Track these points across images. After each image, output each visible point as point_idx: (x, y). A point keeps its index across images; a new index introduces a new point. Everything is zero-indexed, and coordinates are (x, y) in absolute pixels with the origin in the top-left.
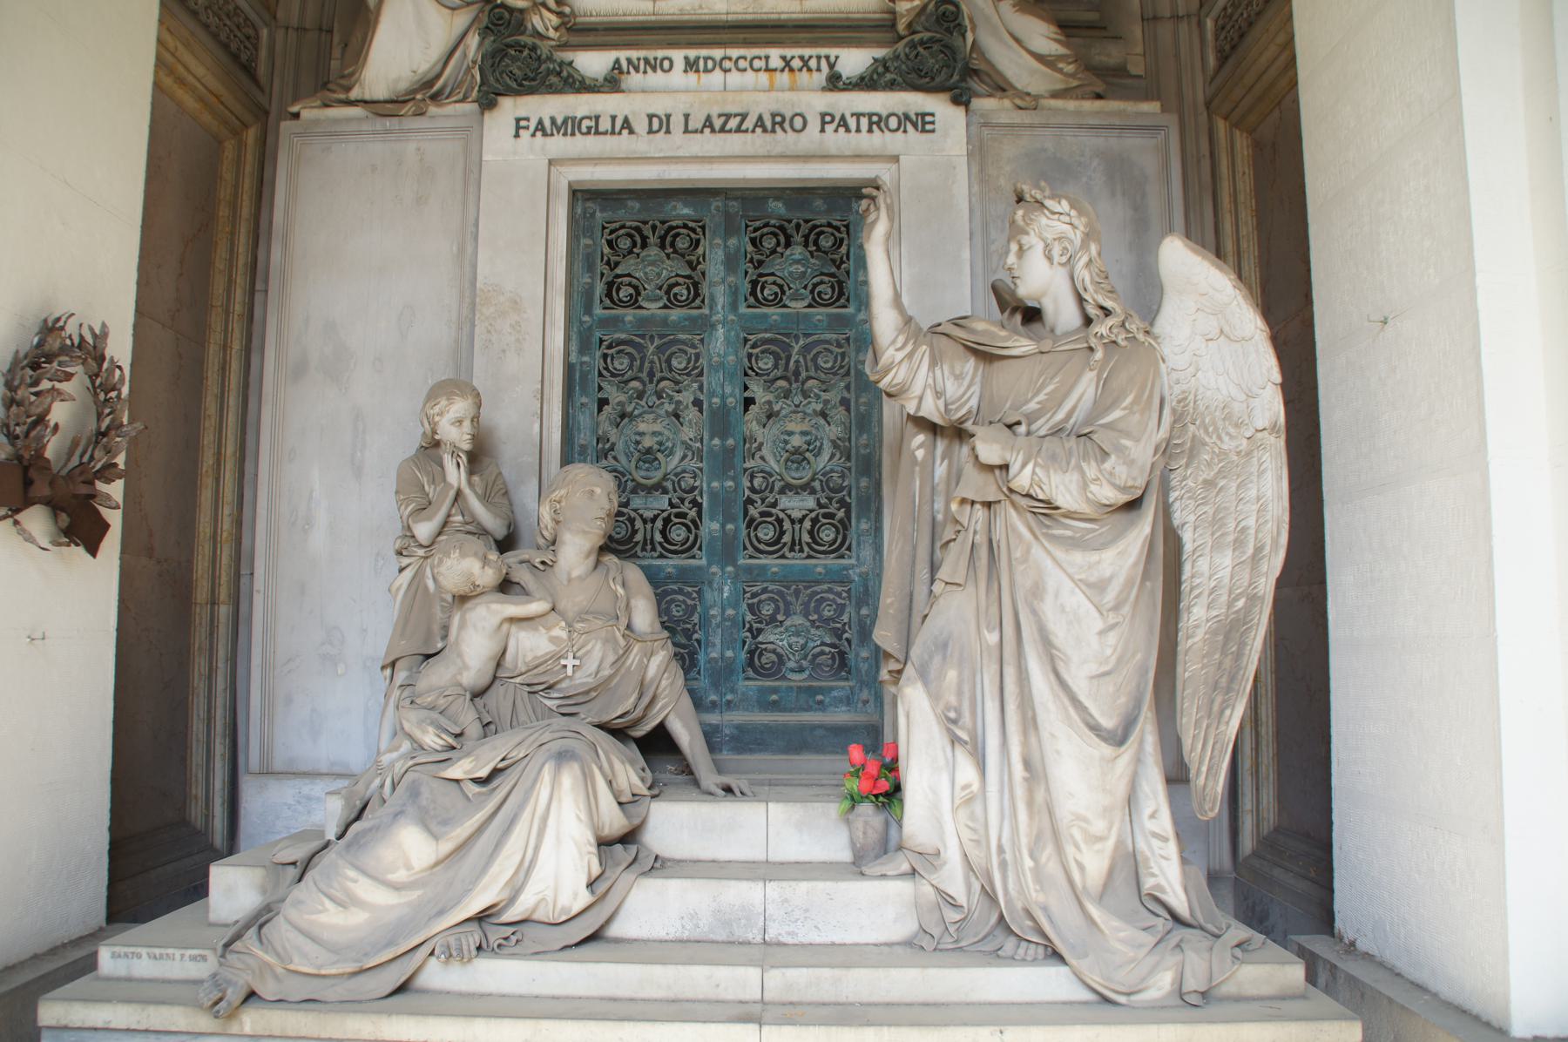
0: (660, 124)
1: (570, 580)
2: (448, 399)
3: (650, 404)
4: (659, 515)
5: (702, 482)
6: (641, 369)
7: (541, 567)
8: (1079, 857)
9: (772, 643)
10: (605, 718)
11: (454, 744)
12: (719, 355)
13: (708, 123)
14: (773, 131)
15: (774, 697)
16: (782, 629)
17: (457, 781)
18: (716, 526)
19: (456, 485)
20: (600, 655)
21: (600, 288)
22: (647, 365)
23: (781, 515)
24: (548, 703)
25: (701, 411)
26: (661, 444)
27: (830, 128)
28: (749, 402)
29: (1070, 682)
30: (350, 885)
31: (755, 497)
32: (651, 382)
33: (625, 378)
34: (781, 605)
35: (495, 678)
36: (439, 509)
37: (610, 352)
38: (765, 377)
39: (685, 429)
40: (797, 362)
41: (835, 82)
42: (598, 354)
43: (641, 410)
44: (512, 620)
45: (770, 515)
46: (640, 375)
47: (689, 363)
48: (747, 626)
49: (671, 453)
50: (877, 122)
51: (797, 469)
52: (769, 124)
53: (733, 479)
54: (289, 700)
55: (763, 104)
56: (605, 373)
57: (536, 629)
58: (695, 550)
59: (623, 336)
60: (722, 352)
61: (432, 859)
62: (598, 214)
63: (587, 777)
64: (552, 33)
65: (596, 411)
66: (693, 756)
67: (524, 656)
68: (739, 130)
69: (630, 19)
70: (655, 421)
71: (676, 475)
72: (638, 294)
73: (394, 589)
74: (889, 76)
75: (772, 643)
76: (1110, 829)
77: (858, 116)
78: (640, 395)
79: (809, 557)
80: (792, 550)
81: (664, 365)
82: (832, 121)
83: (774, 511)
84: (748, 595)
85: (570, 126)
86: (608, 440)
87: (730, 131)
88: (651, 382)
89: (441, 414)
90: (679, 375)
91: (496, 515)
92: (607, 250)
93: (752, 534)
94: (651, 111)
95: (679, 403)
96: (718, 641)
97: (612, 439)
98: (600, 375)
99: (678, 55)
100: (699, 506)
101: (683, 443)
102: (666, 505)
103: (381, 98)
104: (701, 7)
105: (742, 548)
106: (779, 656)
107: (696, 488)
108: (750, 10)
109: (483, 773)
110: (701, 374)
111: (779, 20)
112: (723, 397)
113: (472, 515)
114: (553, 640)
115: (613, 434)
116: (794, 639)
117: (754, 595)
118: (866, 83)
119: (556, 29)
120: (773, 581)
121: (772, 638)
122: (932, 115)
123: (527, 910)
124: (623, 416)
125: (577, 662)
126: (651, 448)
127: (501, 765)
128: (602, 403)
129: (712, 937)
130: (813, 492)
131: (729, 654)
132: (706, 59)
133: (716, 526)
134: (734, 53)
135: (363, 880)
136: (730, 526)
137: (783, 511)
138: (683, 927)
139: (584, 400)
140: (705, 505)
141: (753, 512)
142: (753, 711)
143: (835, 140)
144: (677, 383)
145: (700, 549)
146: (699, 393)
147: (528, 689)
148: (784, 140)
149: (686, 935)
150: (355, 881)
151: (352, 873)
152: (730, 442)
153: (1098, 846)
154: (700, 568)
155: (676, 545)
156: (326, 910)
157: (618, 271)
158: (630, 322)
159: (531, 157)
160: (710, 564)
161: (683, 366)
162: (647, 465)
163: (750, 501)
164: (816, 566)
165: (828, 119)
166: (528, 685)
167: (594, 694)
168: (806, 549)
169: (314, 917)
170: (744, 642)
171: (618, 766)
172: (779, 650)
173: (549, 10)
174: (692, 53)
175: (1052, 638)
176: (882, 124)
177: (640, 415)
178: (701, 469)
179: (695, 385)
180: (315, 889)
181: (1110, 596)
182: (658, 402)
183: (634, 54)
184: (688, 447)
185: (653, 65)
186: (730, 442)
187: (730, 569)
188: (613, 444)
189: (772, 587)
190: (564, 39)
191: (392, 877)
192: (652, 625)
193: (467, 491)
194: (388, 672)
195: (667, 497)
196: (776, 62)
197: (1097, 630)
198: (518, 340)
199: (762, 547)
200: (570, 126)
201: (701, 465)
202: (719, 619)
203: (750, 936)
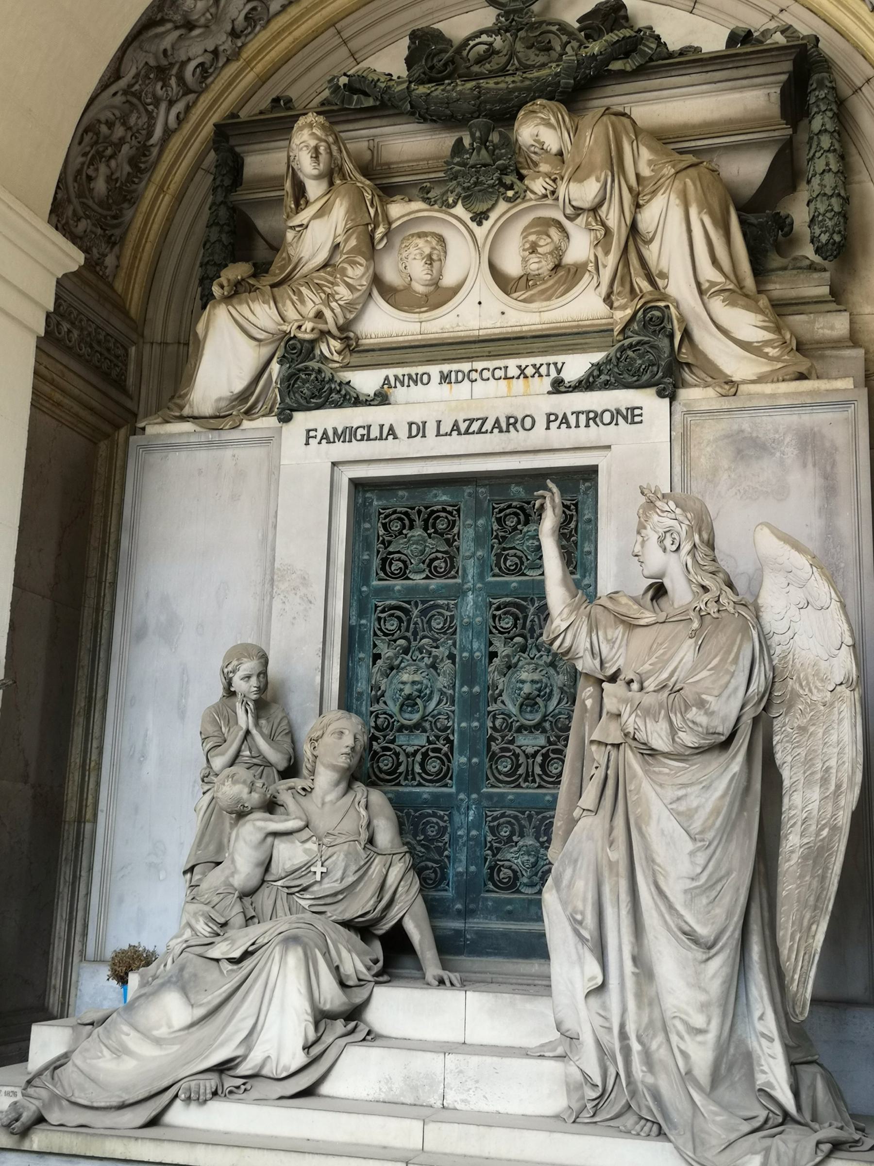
0: (417, 430)
1: (323, 804)
2: (238, 660)
3: (414, 658)
4: (418, 750)
5: (454, 723)
6: (407, 630)
7: (303, 793)
8: (683, 1047)
9: (509, 860)
10: (347, 916)
11: (219, 931)
12: (469, 617)
13: (456, 427)
14: (508, 431)
15: (509, 908)
16: (516, 849)
17: (217, 960)
18: (463, 760)
19: (244, 727)
20: (343, 864)
21: (376, 563)
22: (412, 626)
23: (518, 751)
24: (303, 902)
25: (454, 663)
26: (420, 691)
27: (553, 425)
28: (493, 655)
29: (668, 893)
30: (124, 1037)
31: (496, 735)
32: (415, 640)
33: (394, 638)
34: (516, 827)
35: (263, 881)
36: (230, 746)
37: (383, 615)
38: (506, 635)
39: (441, 678)
40: (532, 621)
41: (558, 386)
42: (374, 617)
43: (406, 663)
44: (276, 834)
45: (509, 750)
46: (407, 634)
47: (445, 624)
48: (488, 845)
49: (430, 698)
50: (594, 418)
51: (531, 712)
52: (504, 425)
53: (478, 720)
55: (499, 411)
56: (379, 633)
57: (293, 842)
58: (448, 780)
59: (393, 602)
60: (471, 615)
61: (188, 1020)
62: (375, 503)
64: (336, 357)
65: (371, 664)
66: (422, 954)
67: (284, 864)
68: (480, 432)
69: (401, 339)
70: (415, 672)
71: (433, 717)
72: (406, 567)
73: (198, 810)
74: (603, 378)
75: (509, 860)
76: (709, 1022)
77: (578, 414)
78: (406, 651)
79: (540, 787)
80: (526, 780)
81: (425, 626)
82: (556, 420)
83: (511, 747)
84: (489, 819)
85: (347, 435)
86: (380, 688)
87: (473, 433)
88: (415, 640)
89: (234, 672)
90: (438, 633)
91: (278, 750)
92: (382, 532)
93: (494, 767)
94: (411, 420)
95: (436, 657)
96: (463, 858)
97: (383, 688)
98: (375, 634)
99: (434, 370)
100: (451, 742)
101: (440, 690)
102: (423, 741)
103: (207, 415)
104: (458, 325)
105: (485, 778)
106: (515, 872)
107: (448, 728)
108: (498, 325)
109: (237, 954)
110: (454, 633)
111: (521, 332)
112: (472, 652)
113: (259, 751)
114: (306, 851)
115: (384, 683)
116: (526, 858)
117: (495, 819)
118: (586, 384)
119: (339, 353)
120: (509, 808)
121: (509, 856)
122: (641, 408)
123: (255, 1066)
124: (392, 669)
125: (324, 870)
126: (410, 695)
127: (250, 949)
128: (377, 657)
129: (402, 1100)
130: (544, 731)
131: (473, 868)
132: (457, 372)
133: (463, 760)
134: (479, 365)
135: (133, 1033)
136: (475, 760)
137: (520, 747)
138: (380, 1089)
139: (362, 655)
140: (456, 742)
141: (494, 747)
142: (491, 920)
143: (559, 436)
144: (435, 640)
145: (451, 779)
146: (453, 649)
147: (286, 890)
148: (517, 439)
149: (382, 1097)
150: (128, 1035)
151: (125, 1028)
152: (477, 689)
153: (700, 1038)
154: (450, 795)
156: (104, 1056)
157: (391, 549)
158: (399, 591)
159: (318, 461)
160: (458, 792)
161: (440, 626)
162: (410, 709)
163: (492, 739)
164: (545, 795)
165: (552, 418)
166: (288, 887)
167: (341, 897)
168: (538, 780)
169: (95, 1061)
170: (486, 859)
171: (345, 953)
172: (514, 867)
173: (334, 337)
174: (446, 368)
175: (655, 856)
176: (598, 420)
177: (405, 667)
178: (453, 712)
179: (450, 642)
180: (98, 1039)
181: (697, 825)
182: (420, 656)
183: (400, 371)
184: (442, 693)
185: (415, 380)
186: (477, 689)
187: (474, 796)
188: (384, 692)
189: (508, 812)
190: (346, 361)
191: (156, 1033)
192: (392, 842)
193: (254, 732)
194: (188, 875)
195: (425, 735)
196: (513, 371)
197: (688, 850)
198: (305, 610)
199: (501, 777)
200: (347, 435)
201: (453, 708)
202: (465, 838)
203: (432, 1101)
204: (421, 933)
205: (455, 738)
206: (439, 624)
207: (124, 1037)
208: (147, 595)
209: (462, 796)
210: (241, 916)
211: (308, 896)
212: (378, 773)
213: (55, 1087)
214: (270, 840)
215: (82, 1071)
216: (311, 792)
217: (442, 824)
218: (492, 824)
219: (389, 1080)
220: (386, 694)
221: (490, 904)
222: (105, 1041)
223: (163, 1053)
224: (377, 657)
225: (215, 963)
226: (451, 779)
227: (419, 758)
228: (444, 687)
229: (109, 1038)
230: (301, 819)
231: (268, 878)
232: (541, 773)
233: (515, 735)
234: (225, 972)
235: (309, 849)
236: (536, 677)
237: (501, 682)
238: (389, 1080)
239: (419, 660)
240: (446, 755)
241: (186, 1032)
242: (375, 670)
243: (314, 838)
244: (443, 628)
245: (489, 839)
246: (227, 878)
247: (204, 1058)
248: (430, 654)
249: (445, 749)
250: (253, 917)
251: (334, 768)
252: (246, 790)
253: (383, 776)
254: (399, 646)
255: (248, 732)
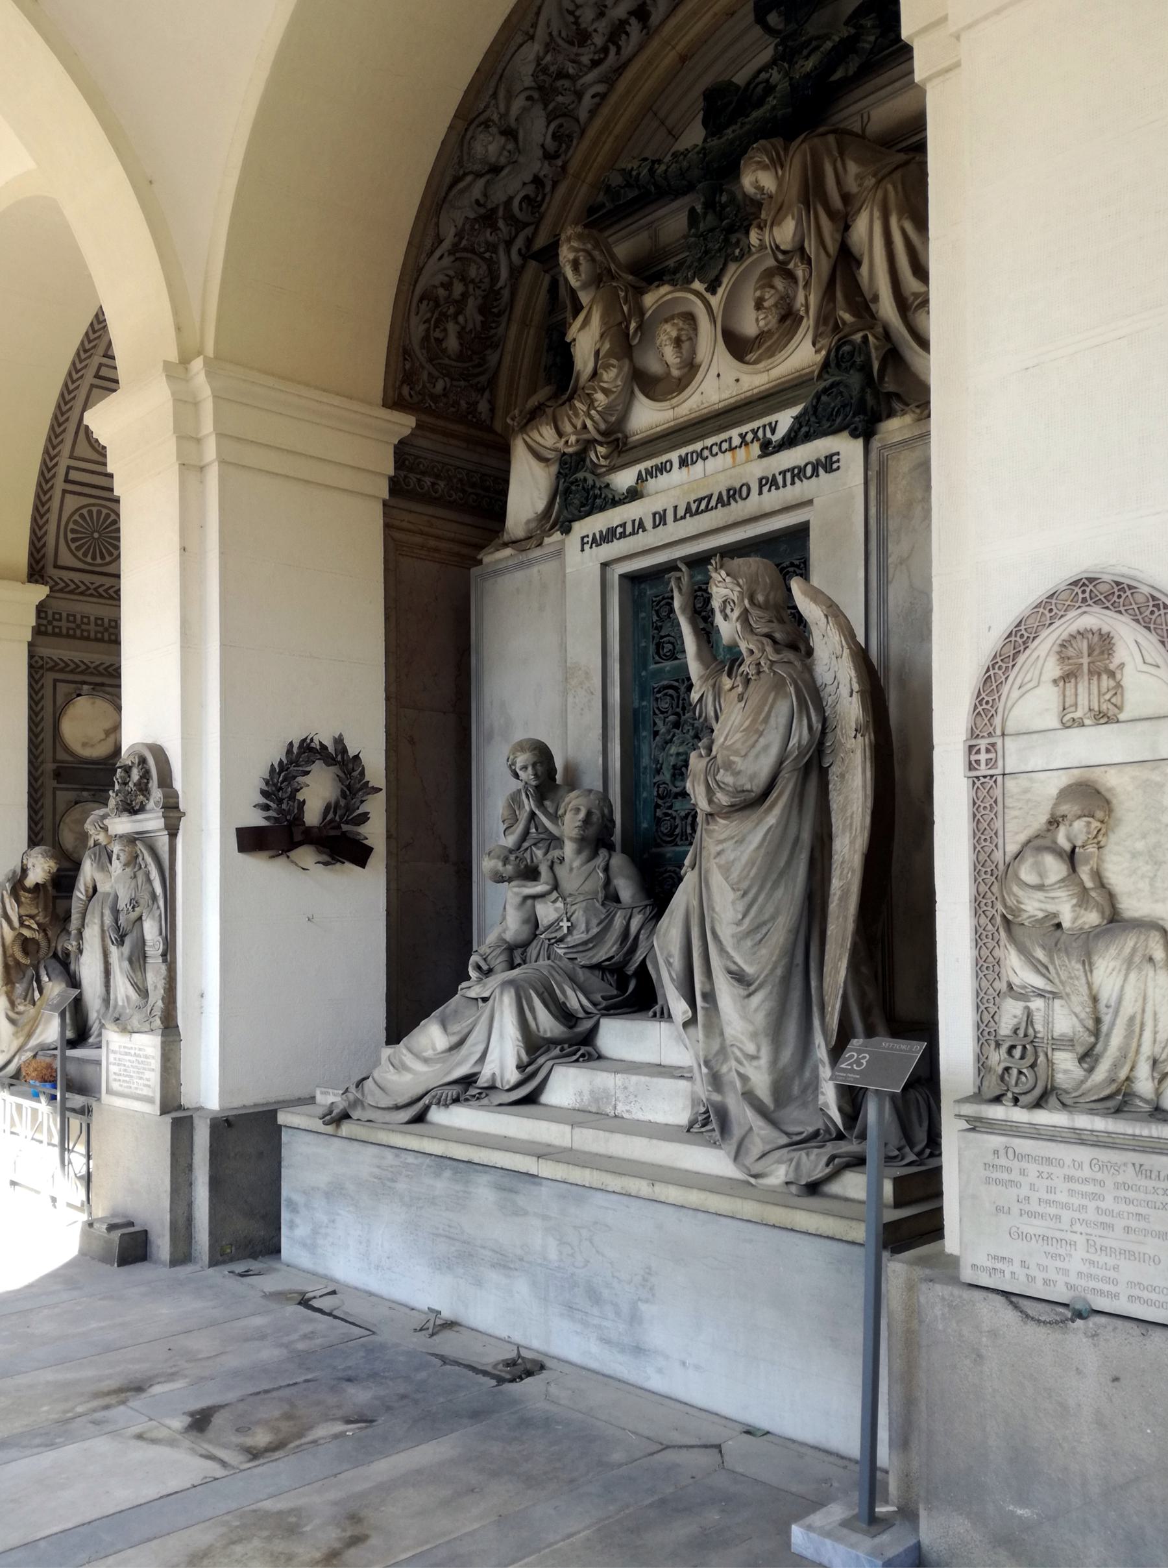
0: (660, 519)
6: (678, 707)
8: (742, 1070)
10: (595, 961)
13: (688, 510)
14: (729, 504)
21: (652, 648)
22: (681, 702)
24: (559, 951)
27: (765, 489)
29: (722, 938)
37: (658, 696)
41: (767, 449)
44: (534, 897)
50: (798, 473)
52: (725, 498)
55: (719, 486)
56: (657, 712)
59: (665, 682)
62: (648, 593)
64: (603, 462)
68: (707, 509)
69: (659, 429)
72: (674, 648)
74: (804, 429)
76: (759, 1050)
77: (783, 473)
82: (766, 484)
85: (609, 536)
87: (702, 512)
92: (655, 618)
94: (654, 510)
98: (655, 714)
99: (674, 456)
103: (522, 538)
104: (702, 403)
108: (734, 394)
111: (746, 398)
114: (556, 910)
118: (790, 441)
119: (605, 458)
122: (838, 454)
124: (667, 743)
125: (569, 924)
128: (656, 733)
132: (692, 453)
134: (709, 442)
139: (644, 734)
143: (772, 499)
148: (738, 509)
149: (577, 1106)
153: (755, 1063)
157: (662, 634)
158: (669, 672)
159: (591, 564)
165: (764, 482)
167: (591, 945)
171: (569, 992)
173: (601, 444)
174: (683, 451)
175: (715, 905)
181: (734, 875)
183: (649, 464)
185: (662, 469)
190: (612, 464)
191: (425, 1054)
192: (633, 897)
193: (537, 812)
196: (736, 441)
197: (730, 900)
198: (589, 701)
200: (609, 536)
208: (492, 703)
219: (581, 1093)
223: (431, 1069)
224: (656, 733)
225: (475, 1001)
238: (581, 1093)
246: (500, 934)
252: (500, 864)
255: (533, 815)
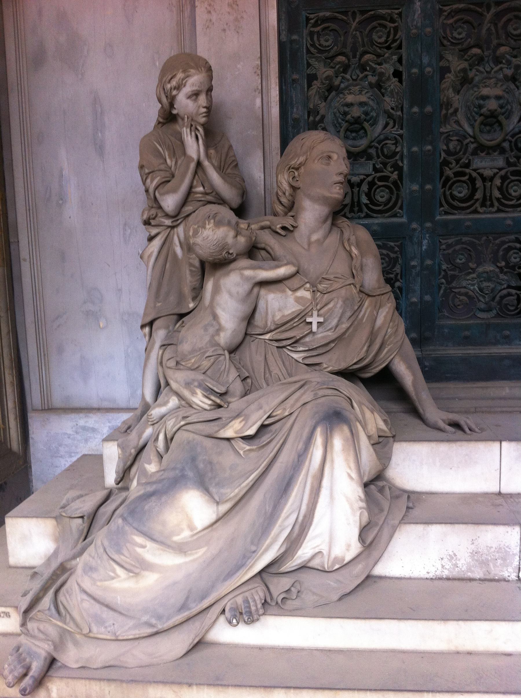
1: (310, 244)
2: (184, 71)
3: (354, 77)
4: (364, 179)
5: (402, 148)
7: (283, 232)
9: (465, 287)
10: (342, 366)
11: (218, 401)
12: (417, 27)
15: (467, 333)
16: (474, 275)
17: (228, 439)
18: (415, 187)
19: (195, 156)
20: (341, 311)
22: (350, 40)
23: (474, 174)
24: (295, 356)
25: (401, 81)
26: (366, 114)
28: (445, 71)
30: (139, 550)
31: (451, 159)
32: (354, 57)
33: (331, 54)
34: (473, 254)
35: (246, 334)
36: (182, 181)
38: (460, 47)
39: (387, 99)
40: (489, 29)
42: (305, 32)
43: (346, 84)
44: (263, 284)
45: (463, 174)
46: (344, 50)
47: (388, 37)
48: (443, 273)
49: (374, 124)
51: (489, 132)
53: (431, 143)
54: (60, 350)
56: (312, 50)
57: (284, 291)
58: (397, 209)
59: (328, 14)
60: (419, 24)
61: (213, 517)
63: (354, 435)
65: (306, 86)
66: (417, 394)
67: (273, 316)
70: (360, 92)
71: (379, 142)
73: (146, 257)
75: (465, 287)
78: (346, 68)
79: (499, 211)
80: (483, 205)
81: (366, 40)
83: (467, 171)
84: (444, 247)
86: (318, 113)
88: (354, 57)
89: (178, 88)
90: (380, 48)
91: (232, 185)
93: (448, 193)
95: (381, 74)
96: (417, 288)
97: (322, 112)
98: (308, 51)
100: (400, 169)
101: (386, 112)
102: (369, 169)
105: (438, 205)
106: (469, 297)
107: (395, 154)
109: (251, 431)
110: (400, 47)
112: (421, 68)
113: (212, 187)
114: (298, 300)
115: (322, 107)
116: (485, 284)
117: (449, 246)
120: (466, 234)
121: (464, 283)
123: (305, 561)
125: (321, 320)
126: (359, 117)
127: (266, 423)
128: (312, 78)
129: (470, 575)
130: (503, 151)
131: (427, 298)
133: (415, 187)
135: (149, 544)
136: (428, 187)
137: (475, 170)
138: (443, 566)
139: (295, 76)
140: (405, 168)
141: (449, 172)
142: (447, 346)
144: (379, 56)
145: (401, 208)
146: (398, 65)
147: (277, 344)
149: (446, 573)
150: (143, 547)
151: (139, 539)
152: (429, 109)
154: (401, 225)
155: (380, 205)
156: (118, 576)
160: (410, 221)
161: (383, 40)
162: (354, 134)
163: (446, 163)
164: (505, 219)
166: (277, 341)
168: (496, 204)
169: (107, 583)
170: (440, 288)
172: (471, 293)
177: (346, 88)
178: (401, 136)
179: (395, 58)
180: (105, 557)
182: (361, 76)
184: (390, 116)
186: (429, 109)
187: (428, 225)
188: (323, 117)
189: (465, 239)
192: (378, 281)
193: (206, 163)
194: (147, 330)
195: (371, 162)
198: (236, 20)
199: (456, 203)
201: (401, 132)
202: (418, 268)
203: (506, 574)
204: (414, 374)
205: (405, 165)
206: (380, 37)
207: (139, 550)
208: (40, 13)
209: (414, 225)
210: (239, 381)
211: (301, 349)
212: (451, 201)
213: (65, 623)
214: (256, 290)
215: (94, 599)
216: (292, 231)
217: (392, 255)
218: (446, 252)
219: (452, 557)
220: (326, 120)
221: (446, 330)
222: (116, 557)
223: (188, 559)
224: (312, 78)
225: (226, 443)
226: (401, 208)
227: (365, 187)
228: (392, 109)
229: (119, 552)
230: (294, 265)
231: (251, 331)
232: (500, 196)
233: (471, 158)
234: (241, 453)
235: (302, 298)
236: (498, 91)
237: (457, 100)
238: (452, 557)
239: (361, 79)
240: (395, 183)
241: (210, 529)
242: (313, 91)
243: (308, 285)
244: (386, 42)
245: (444, 267)
246: (213, 336)
247: (249, 569)
248: (374, 72)
249: (395, 176)
250: (248, 377)
251: (324, 200)
252: (232, 234)
253: (456, 203)
254: (339, 63)
255: (199, 164)
